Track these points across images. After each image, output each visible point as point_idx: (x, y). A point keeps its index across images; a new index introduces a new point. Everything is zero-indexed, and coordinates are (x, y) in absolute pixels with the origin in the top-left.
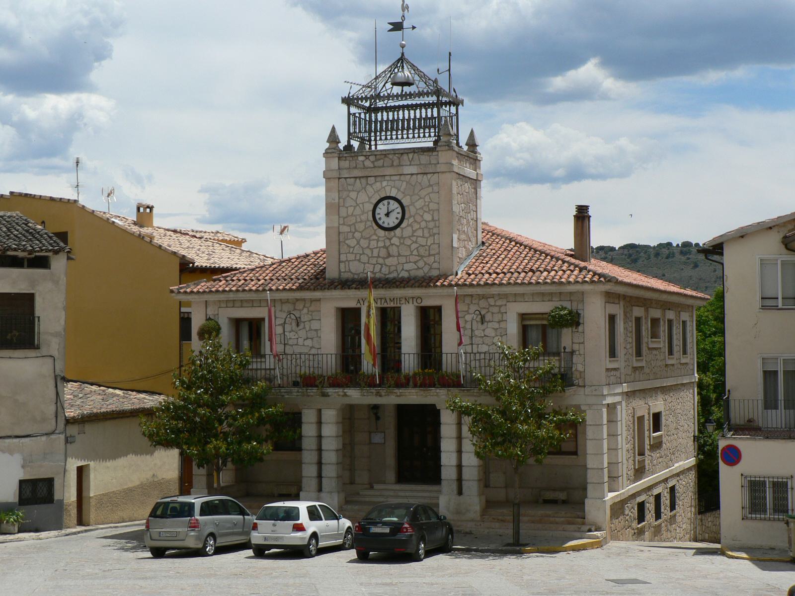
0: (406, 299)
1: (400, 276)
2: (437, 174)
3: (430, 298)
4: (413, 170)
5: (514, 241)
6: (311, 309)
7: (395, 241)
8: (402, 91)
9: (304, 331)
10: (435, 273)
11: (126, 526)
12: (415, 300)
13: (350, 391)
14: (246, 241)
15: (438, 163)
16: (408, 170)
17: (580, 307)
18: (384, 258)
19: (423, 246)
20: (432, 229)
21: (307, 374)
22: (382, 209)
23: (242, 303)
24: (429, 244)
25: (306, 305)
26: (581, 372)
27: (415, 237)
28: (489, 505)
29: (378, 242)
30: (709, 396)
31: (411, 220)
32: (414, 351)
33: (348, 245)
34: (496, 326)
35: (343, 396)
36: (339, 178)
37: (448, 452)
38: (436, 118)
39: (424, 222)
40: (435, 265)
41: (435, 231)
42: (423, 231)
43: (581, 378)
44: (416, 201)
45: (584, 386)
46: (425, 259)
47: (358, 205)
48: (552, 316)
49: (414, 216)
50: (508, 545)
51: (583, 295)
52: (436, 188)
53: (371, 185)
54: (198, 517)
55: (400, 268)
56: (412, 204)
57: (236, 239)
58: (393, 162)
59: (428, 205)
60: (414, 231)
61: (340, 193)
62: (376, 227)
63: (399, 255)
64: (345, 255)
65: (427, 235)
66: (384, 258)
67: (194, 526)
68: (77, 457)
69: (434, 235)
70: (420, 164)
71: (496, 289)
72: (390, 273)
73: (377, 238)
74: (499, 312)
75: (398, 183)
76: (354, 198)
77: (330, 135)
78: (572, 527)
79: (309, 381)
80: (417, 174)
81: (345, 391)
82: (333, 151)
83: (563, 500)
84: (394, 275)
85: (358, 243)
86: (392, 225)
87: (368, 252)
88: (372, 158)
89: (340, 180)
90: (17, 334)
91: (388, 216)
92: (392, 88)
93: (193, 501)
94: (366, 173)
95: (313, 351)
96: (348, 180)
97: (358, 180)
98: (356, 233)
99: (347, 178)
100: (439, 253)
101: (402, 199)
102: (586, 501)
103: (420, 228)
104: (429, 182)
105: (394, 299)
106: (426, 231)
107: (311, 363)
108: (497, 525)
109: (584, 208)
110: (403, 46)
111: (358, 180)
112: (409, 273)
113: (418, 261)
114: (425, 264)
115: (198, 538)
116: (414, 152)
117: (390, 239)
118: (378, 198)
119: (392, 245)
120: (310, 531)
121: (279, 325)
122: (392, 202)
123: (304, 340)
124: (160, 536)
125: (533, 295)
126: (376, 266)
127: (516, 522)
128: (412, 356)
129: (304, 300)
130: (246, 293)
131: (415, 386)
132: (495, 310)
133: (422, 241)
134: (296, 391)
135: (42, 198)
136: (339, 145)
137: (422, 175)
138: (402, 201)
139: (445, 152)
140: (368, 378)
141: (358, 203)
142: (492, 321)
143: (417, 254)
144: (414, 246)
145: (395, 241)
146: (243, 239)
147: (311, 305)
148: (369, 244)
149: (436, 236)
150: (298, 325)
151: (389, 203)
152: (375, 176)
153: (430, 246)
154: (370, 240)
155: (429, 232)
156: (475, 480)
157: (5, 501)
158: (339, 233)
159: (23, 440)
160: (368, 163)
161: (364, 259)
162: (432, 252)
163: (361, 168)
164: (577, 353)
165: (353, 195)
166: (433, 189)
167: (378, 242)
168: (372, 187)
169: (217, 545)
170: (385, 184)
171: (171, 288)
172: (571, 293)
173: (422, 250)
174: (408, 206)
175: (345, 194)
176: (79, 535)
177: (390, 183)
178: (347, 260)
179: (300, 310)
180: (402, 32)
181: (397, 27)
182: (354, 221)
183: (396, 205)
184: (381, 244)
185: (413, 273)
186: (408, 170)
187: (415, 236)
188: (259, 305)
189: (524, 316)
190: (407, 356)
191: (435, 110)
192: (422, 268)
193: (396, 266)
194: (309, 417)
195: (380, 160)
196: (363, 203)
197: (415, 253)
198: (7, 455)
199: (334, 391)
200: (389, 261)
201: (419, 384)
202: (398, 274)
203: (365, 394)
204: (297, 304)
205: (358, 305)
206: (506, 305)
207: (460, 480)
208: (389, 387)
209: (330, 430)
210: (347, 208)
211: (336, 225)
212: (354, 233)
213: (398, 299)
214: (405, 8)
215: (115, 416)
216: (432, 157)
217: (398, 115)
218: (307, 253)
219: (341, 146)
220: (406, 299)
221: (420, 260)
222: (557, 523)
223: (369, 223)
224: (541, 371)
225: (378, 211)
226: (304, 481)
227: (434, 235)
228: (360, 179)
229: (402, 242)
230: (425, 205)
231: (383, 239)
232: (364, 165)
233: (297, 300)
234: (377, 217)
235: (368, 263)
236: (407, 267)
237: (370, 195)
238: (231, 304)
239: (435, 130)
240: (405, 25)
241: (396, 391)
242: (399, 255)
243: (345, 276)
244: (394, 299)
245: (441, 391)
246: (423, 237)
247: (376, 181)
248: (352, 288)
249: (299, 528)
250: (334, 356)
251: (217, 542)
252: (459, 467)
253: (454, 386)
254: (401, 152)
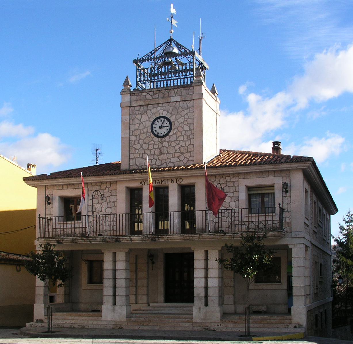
0: (172, 180)
2: (193, 100)
4: (178, 99)
7: (165, 144)
9: (106, 203)
12: (178, 180)
16: (174, 99)
18: (158, 156)
20: (189, 135)
22: (158, 124)
24: (187, 145)
25: (108, 187)
26: (288, 223)
27: (178, 141)
28: (224, 315)
29: (154, 145)
31: (176, 130)
33: (134, 148)
34: (232, 195)
40: (191, 158)
42: (183, 137)
47: (142, 123)
49: (178, 128)
53: (150, 110)
55: (168, 161)
58: (164, 95)
59: (187, 120)
60: (177, 138)
62: (153, 136)
63: (168, 153)
64: (133, 155)
65: (186, 139)
66: (158, 156)
69: (191, 139)
72: (161, 165)
73: (153, 143)
74: (234, 186)
75: (167, 108)
77: (125, 81)
81: (131, 237)
85: (141, 147)
88: (151, 93)
89: (131, 108)
98: (140, 140)
99: (136, 106)
103: (181, 135)
105: (164, 180)
106: (185, 137)
113: (179, 156)
117: (162, 143)
119: (163, 147)
121: (90, 200)
123: (106, 208)
132: (231, 184)
133: (183, 143)
141: (142, 121)
142: (229, 192)
145: (165, 144)
147: (110, 187)
148: (149, 146)
153: (188, 146)
155: (187, 138)
158: (130, 141)
160: (149, 97)
162: (189, 150)
164: (286, 210)
167: (154, 145)
170: (159, 108)
173: (182, 150)
174: (174, 122)
175: (134, 116)
177: (162, 108)
178: (134, 158)
182: (139, 133)
184: (156, 147)
186: (174, 99)
188: (78, 188)
192: (182, 161)
195: (156, 94)
196: (145, 122)
197: (178, 151)
206: (238, 181)
207: (206, 296)
210: (135, 125)
212: (139, 140)
213: (167, 180)
216: (189, 90)
220: (172, 180)
221: (181, 155)
223: (148, 134)
226: (105, 298)
230: (185, 121)
232: (146, 98)
236: (173, 160)
242: (168, 153)
243: (132, 167)
244: (164, 180)
246: (183, 141)
252: (206, 288)
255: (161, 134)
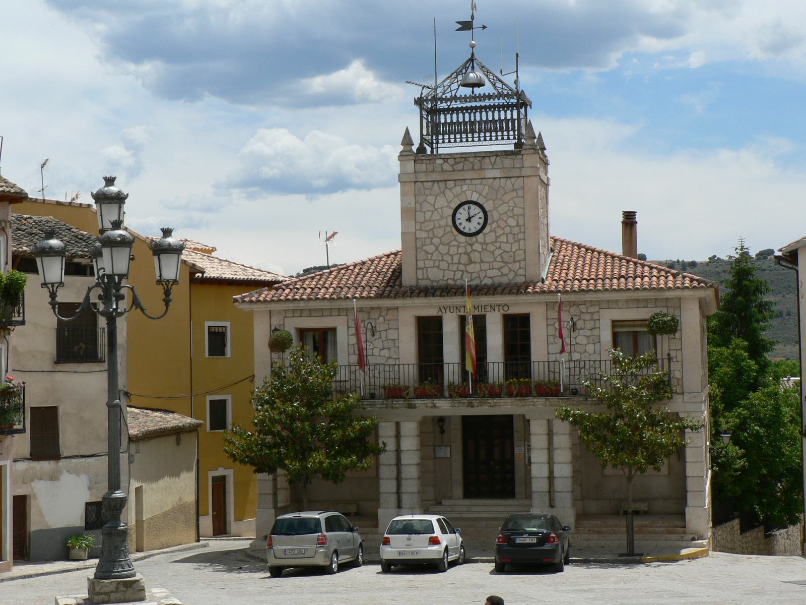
0: (491, 307)
1: (483, 283)
2: (521, 178)
3: (518, 305)
4: (497, 173)
5: (584, 247)
6: (387, 318)
7: (477, 247)
8: (473, 92)
9: (380, 341)
10: (520, 280)
11: (185, 550)
12: (501, 307)
13: (440, 402)
14: (216, 250)
15: (523, 167)
16: (490, 174)
17: (677, 313)
18: (465, 265)
19: (507, 252)
20: (517, 234)
21: (547, 379)
22: (462, 214)
23: (311, 312)
24: (513, 250)
25: (382, 314)
26: (678, 379)
27: (499, 243)
29: (458, 248)
30: (717, 407)
31: (494, 225)
32: (414, 362)
33: (425, 251)
34: (589, 333)
35: (431, 407)
36: (415, 182)
37: (539, 463)
38: (503, 120)
39: (508, 227)
40: (521, 272)
41: (521, 236)
42: (507, 237)
43: (678, 385)
44: (500, 206)
45: (683, 393)
46: (510, 266)
47: (436, 210)
48: (655, 323)
49: (497, 222)
50: (621, 555)
51: (680, 301)
52: (520, 193)
53: (450, 189)
54: (325, 533)
55: (482, 275)
56: (495, 208)
57: (207, 248)
58: (473, 166)
59: (513, 210)
60: (497, 237)
61: (417, 197)
62: (456, 233)
63: (482, 261)
64: (423, 262)
65: (511, 240)
66: (465, 265)
67: (322, 542)
68: (139, 479)
69: (519, 240)
70: (503, 168)
71: (591, 296)
72: (471, 280)
73: (457, 244)
74: (592, 319)
75: (479, 188)
76: (433, 203)
77: (405, 137)
78: (675, 536)
79: (394, 393)
80: (500, 178)
81: (435, 402)
82: (409, 153)
83: (645, 511)
84: (477, 282)
85: (437, 249)
86: (473, 230)
87: (448, 258)
89: (417, 184)
90: (84, 346)
91: (470, 221)
92: (457, 89)
93: (318, 517)
94: (445, 177)
95: (391, 362)
96: (425, 184)
97: (436, 184)
98: (435, 239)
99: (425, 181)
100: (525, 259)
101: (484, 203)
102: (687, 509)
103: (504, 234)
104: (513, 186)
105: (478, 307)
106: (510, 236)
107: (387, 374)
108: (595, 536)
109: (632, 214)
110: (473, 47)
111: (436, 184)
112: (493, 280)
113: (502, 267)
114: (510, 271)
115: (326, 555)
116: (497, 156)
117: (472, 245)
118: (459, 203)
119: (474, 251)
120: (444, 544)
121: (352, 335)
122: (473, 206)
123: (380, 350)
124: (285, 554)
125: (627, 301)
126: (457, 273)
127: (630, 532)
128: (411, 367)
129: (380, 308)
130: (318, 301)
131: (510, 395)
132: (588, 317)
133: (507, 247)
134: (380, 403)
135: (46, 202)
136: (413, 147)
137: (506, 179)
138: (484, 206)
139: (530, 156)
140: (460, 388)
141: (436, 207)
142: (584, 329)
143: (501, 260)
144: (497, 252)
145: (477, 247)
146: (213, 248)
147: (387, 314)
148: (449, 250)
149: (522, 242)
150: (373, 335)
151: (469, 208)
152: (455, 180)
153: (514, 252)
154: (450, 246)
155: (514, 238)
156: (568, 492)
157: (72, 526)
158: (416, 239)
159: (89, 460)
160: (446, 167)
161: (444, 265)
162: (517, 258)
163: (439, 172)
164: (675, 360)
165: (431, 199)
166: (517, 193)
167: (458, 248)
168: (451, 191)
169: (339, 562)
170: (465, 188)
171: (234, 297)
172: (667, 299)
173: (506, 256)
174: (491, 211)
175: (421, 199)
176: (145, 560)
177: (470, 187)
178: (425, 267)
179: (376, 319)
180: (471, 31)
181: (466, 26)
182: (432, 227)
183: (478, 209)
184: (461, 250)
185: (497, 280)
186: (490, 174)
187: (498, 242)
188: (330, 314)
189: (614, 323)
190: (536, 364)
191: (515, 112)
192: (506, 275)
193: (478, 273)
194: (386, 432)
195: (459, 163)
196: (441, 208)
197: (499, 259)
198: (74, 476)
199: (423, 402)
200: (470, 268)
201: (515, 394)
202: (481, 282)
203: (456, 405)
204: (372, 312)
205: (440, 314)
206: (599, 312)
207: (551, 492)
208: (484, 397)
209: (410, 443)
210: (424, 212)
211: (413, 230)
212: (432, 239)
213: (483, 307)
214: (474, 7)
215: (161, 434)
216: (515, 160)
217: (475, 117)
218: (364, 260)
219: (415, 148)
220: (491, 307)
221: (504, 266)
222: (657, 533)
223: (448, 229)
224: (655, 378)
225: (458, 216)
226: (382, 497)
227: (519, 240)
228: (438, 183)
229: (484, 247)
230: (509, 210)
231: (464, 245)
232: (442, 168)
233: (372, 308)
234: (458, 222)
235: (448, 270)
236: (490, 273)
237: (449, 200)
238: (298, 314)
239: (514, 133)
240: (475, 25)
241: (490, 401)
242: (482, 261)
243: (423, 283)
244: (478, 307)
245: (539, 400)
246: (507, 242)
247: (455, 185)
248: (437, 296)
249: (435, 541)
250: (501, 366)
251: (339, 559)
252: (551, 478)
253: (552, 395)
254: (483, 155)
255: (464, 228)
